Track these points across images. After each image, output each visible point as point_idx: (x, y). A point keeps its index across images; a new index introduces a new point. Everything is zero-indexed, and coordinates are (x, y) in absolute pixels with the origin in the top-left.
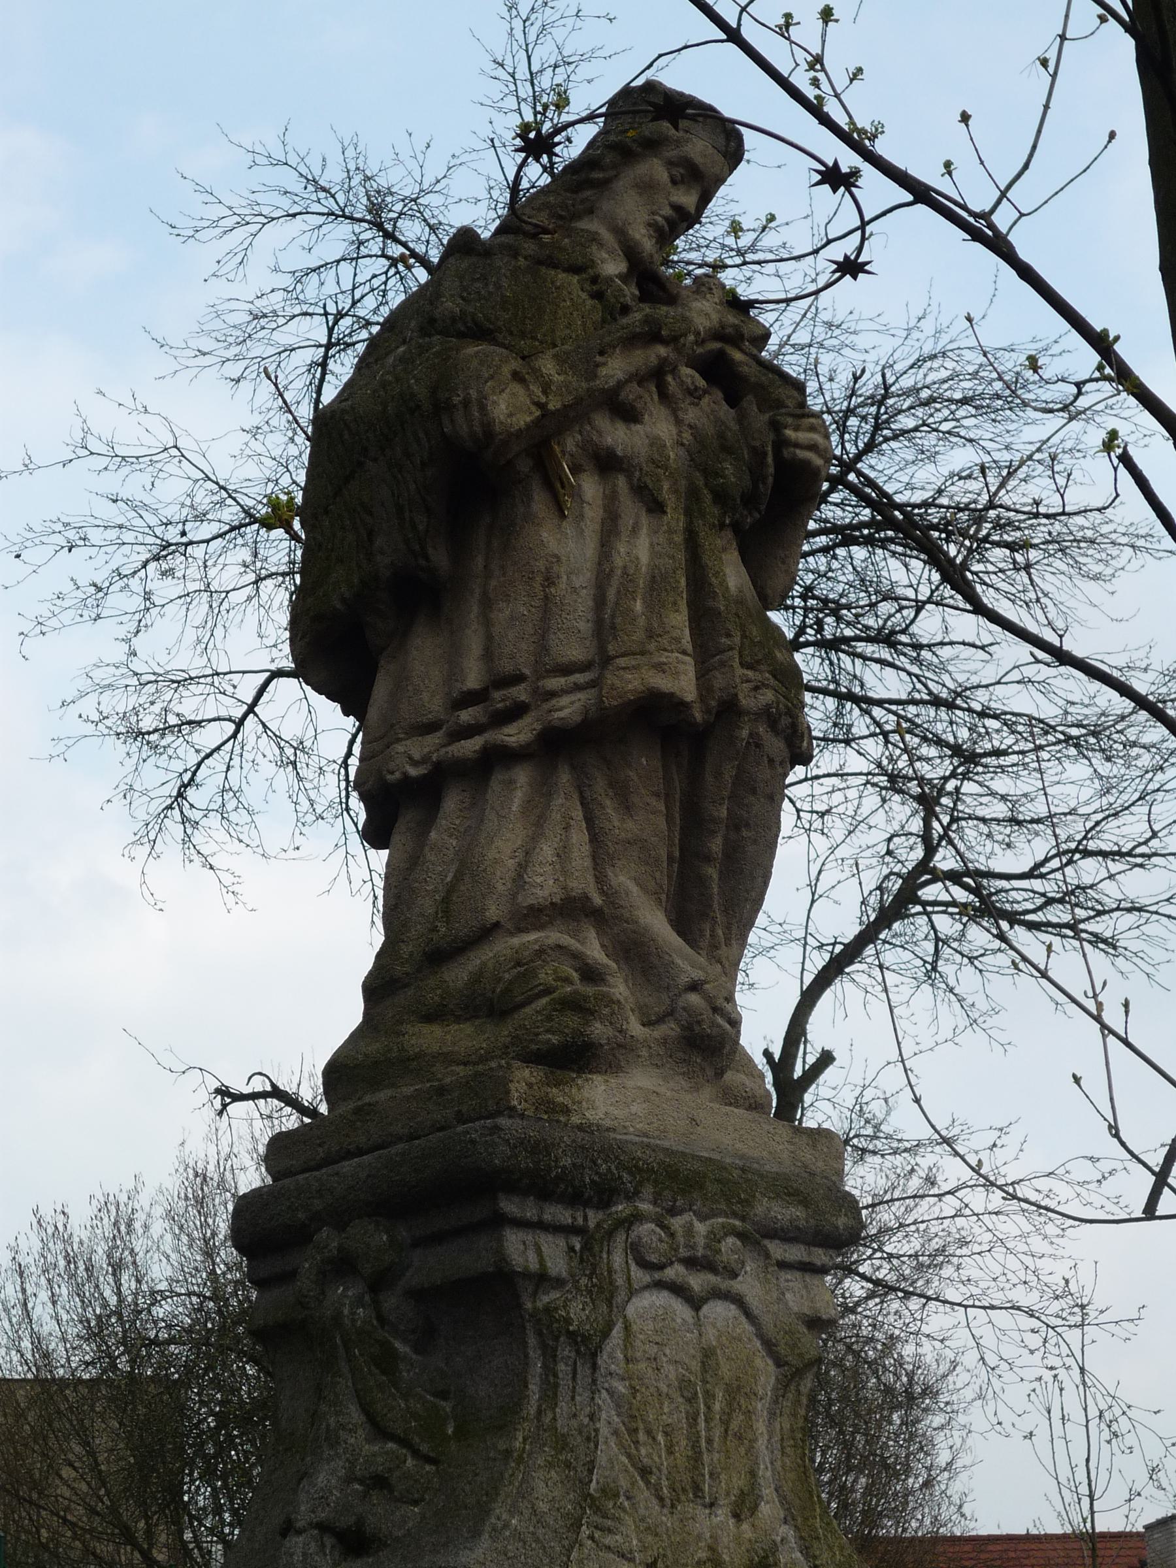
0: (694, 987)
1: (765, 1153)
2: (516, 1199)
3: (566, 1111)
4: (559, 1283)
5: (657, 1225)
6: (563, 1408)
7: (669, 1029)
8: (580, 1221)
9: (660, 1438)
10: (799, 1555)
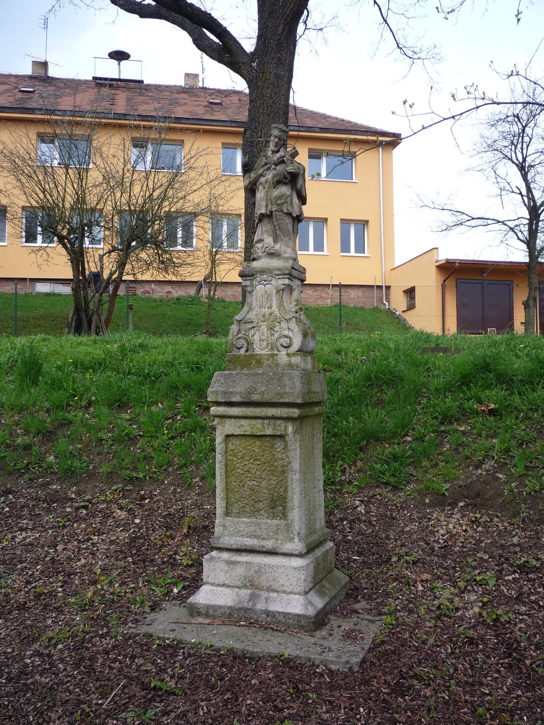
0: (267, 248)
7: (265, 253)
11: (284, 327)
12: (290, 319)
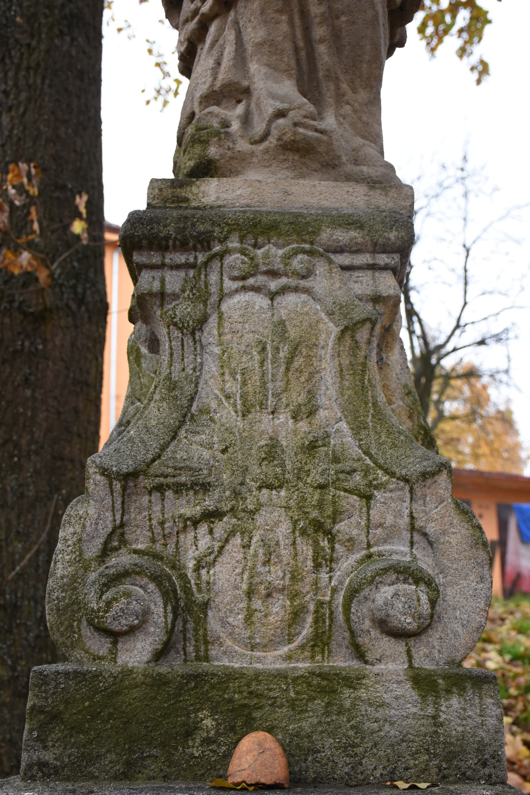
1: (344, 205)
2: (145, 253)
3: (187, 200)
4: (175, 296)
5: (242, 254)
6: (177, 366)
8: (192, 260)
9: (239, 377)
10: (350, 439)
11: (389, 520)
12: (425, 475)
